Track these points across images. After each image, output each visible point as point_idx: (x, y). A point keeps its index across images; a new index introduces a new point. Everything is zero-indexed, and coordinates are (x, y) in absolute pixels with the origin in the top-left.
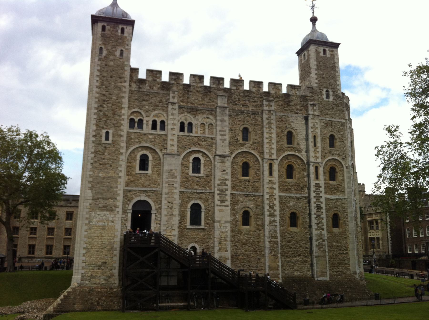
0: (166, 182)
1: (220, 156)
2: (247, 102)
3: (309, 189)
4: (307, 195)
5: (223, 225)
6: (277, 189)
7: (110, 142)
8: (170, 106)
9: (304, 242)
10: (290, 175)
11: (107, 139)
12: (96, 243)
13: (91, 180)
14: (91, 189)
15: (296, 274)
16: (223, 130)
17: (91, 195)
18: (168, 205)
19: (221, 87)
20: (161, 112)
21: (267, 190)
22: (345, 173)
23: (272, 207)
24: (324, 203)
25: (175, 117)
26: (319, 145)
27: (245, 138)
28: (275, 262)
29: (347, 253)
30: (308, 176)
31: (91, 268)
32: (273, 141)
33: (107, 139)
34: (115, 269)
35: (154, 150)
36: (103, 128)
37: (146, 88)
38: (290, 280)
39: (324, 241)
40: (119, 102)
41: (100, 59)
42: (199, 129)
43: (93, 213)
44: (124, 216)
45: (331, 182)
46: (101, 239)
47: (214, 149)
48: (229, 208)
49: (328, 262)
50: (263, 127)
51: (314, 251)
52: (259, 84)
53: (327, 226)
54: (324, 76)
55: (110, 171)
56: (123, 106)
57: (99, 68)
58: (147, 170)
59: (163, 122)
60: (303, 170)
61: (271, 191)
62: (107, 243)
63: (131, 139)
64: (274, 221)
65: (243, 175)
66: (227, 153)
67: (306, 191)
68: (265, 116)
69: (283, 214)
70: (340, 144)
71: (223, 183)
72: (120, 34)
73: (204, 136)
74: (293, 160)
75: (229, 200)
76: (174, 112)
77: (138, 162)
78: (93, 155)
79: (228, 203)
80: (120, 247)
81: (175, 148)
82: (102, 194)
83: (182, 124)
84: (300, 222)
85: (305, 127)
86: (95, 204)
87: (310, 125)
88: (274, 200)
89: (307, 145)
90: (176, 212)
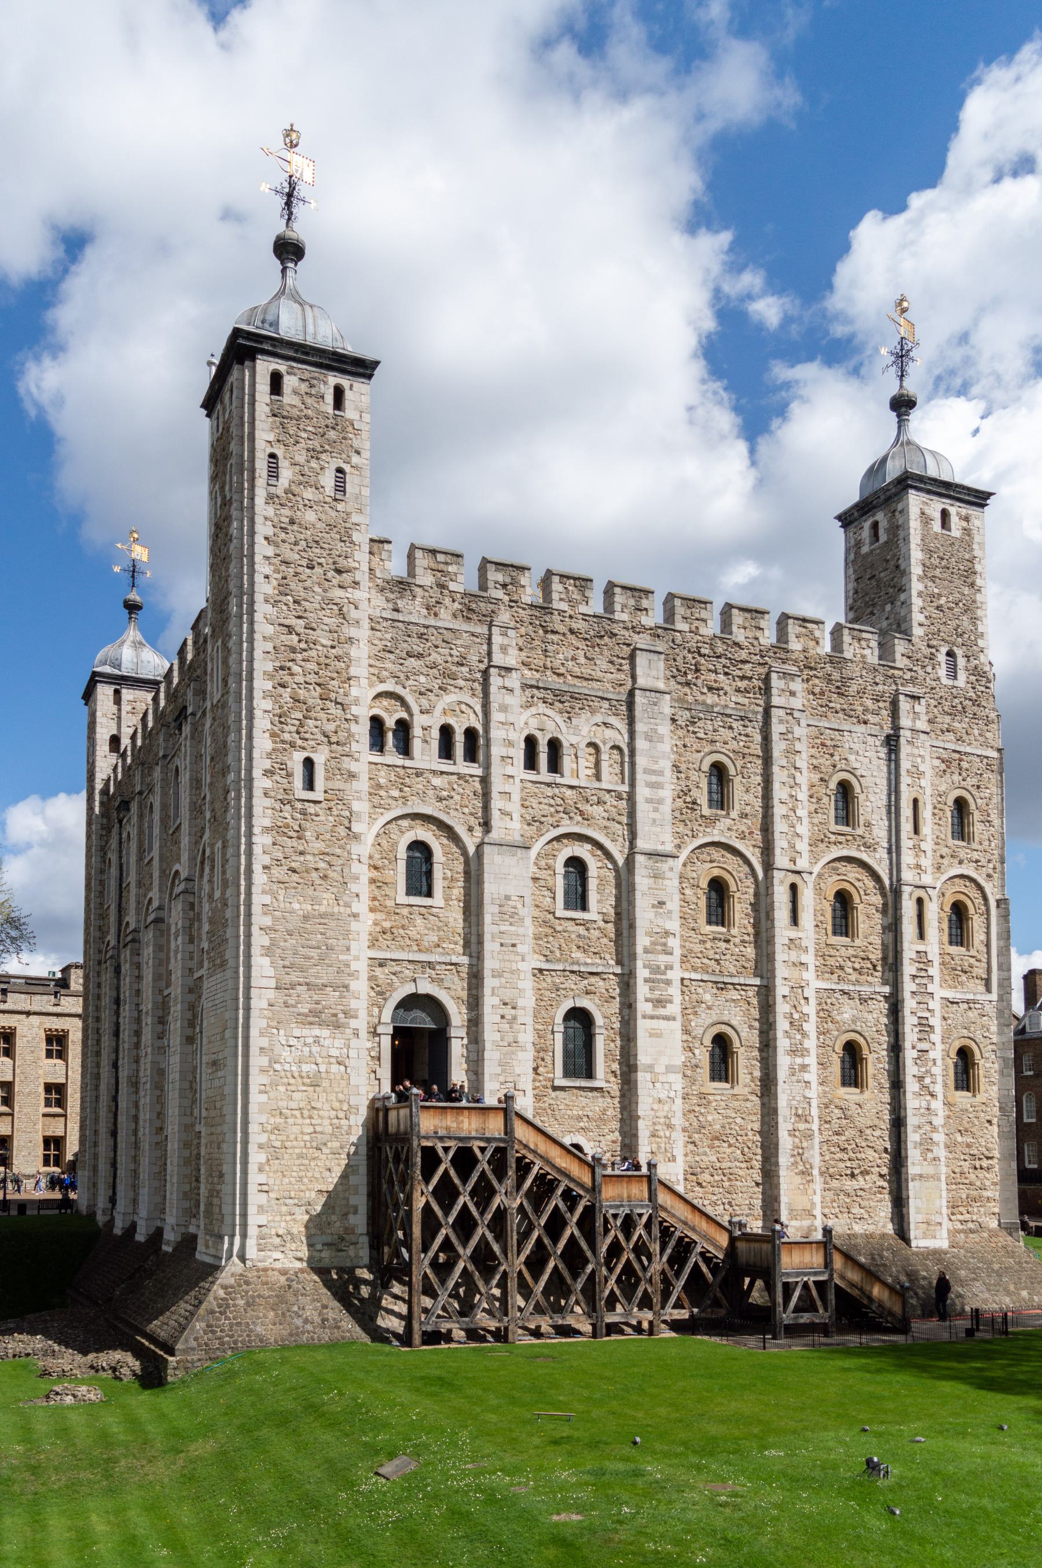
1: (650, 855)
6: (812, 968)
12: (296, 1129)
13: (270, 924)
14: (268, 952)
15: (858, 1228)
16: (655, 767)
17: (271, 972)
18: (501, 1012)
20: (466, 698)
23: (796, 1025)
24: (938, 1014)
26: (926, 829)
31: (284, 1209)
32: (799, 813)
34: (356, 1212)
39: (935, 1129)
43: (282, 1032)
45: (955, 950)
46: (311, 1117)
48: (677, 1025)
51: (910, 1160)
53: (945, 1085)
55: (325, 895)
58: (429, 894)
63: (380, 786)
64: (804, 1068)
66: (669, 848)
68: (777, 728)
73: (597, 785)
74: (853, 873)
75: (677, 999)
77: (402, 866)
79: (674, 1009)
80: (368, 1143)
83: (531, 742)
86: (286, 1005)
88: (802, 1002)
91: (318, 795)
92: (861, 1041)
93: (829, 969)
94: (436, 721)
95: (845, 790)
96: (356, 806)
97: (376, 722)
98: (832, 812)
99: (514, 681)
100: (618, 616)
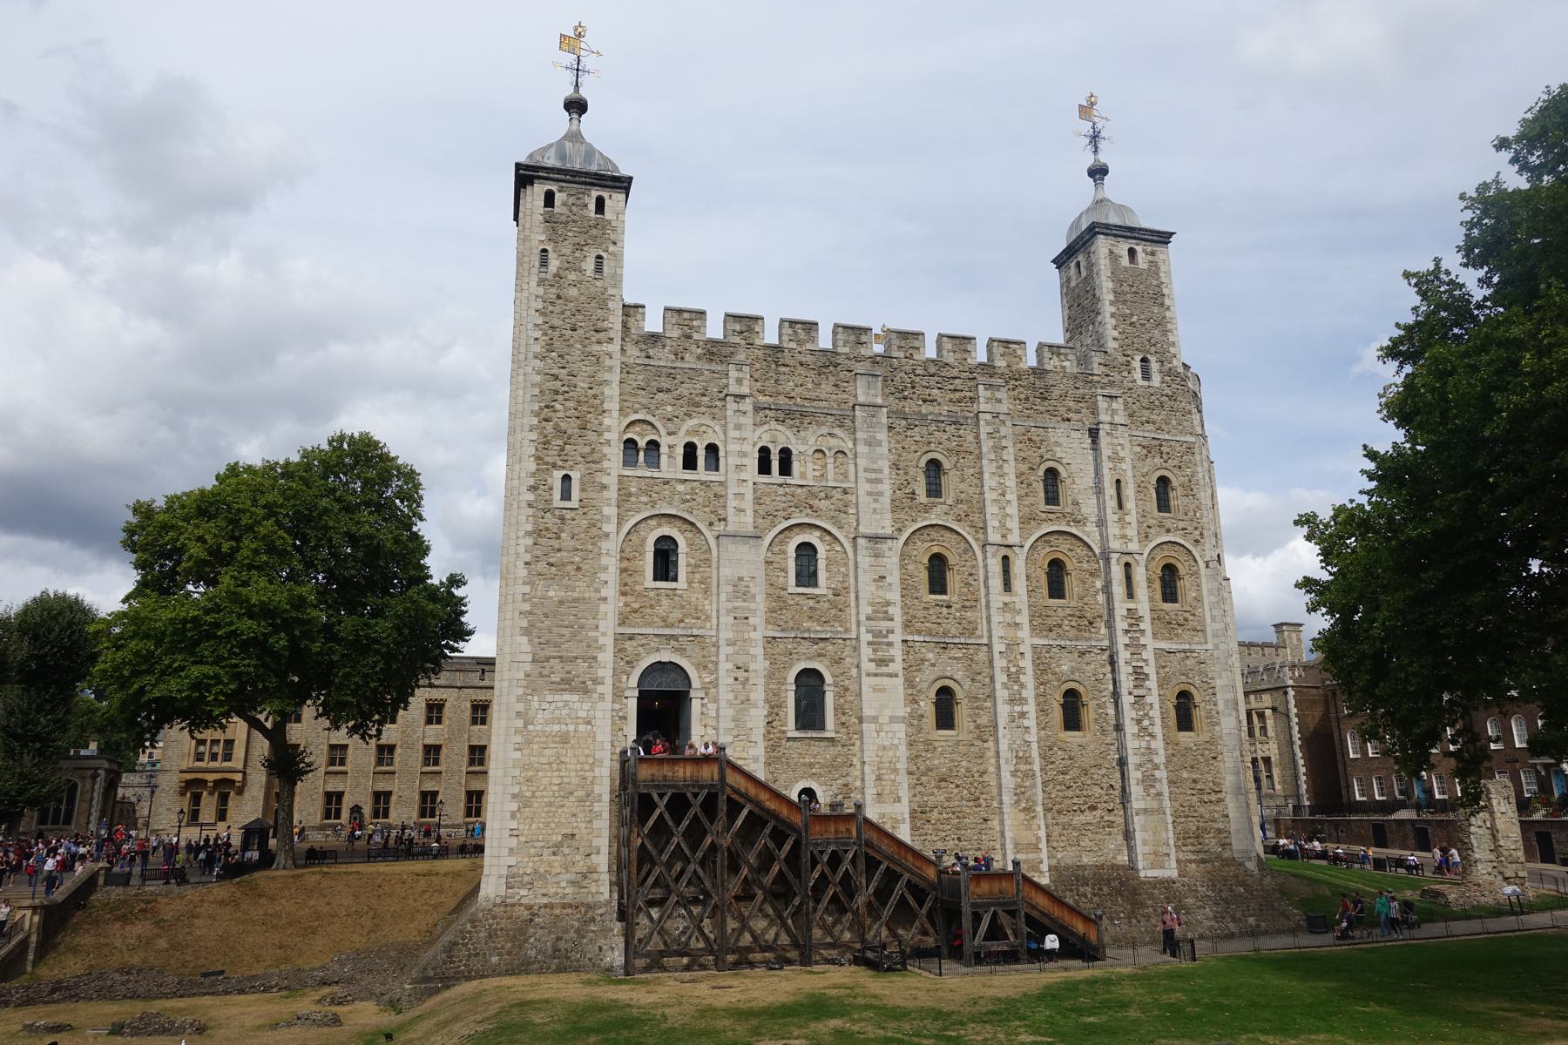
0: (728, 611)
2: (936, 391)
3: (1110, 625)
4: (1106, 643)
5: (886, 728)
6: (1026, 626)
7: (574, 503)
8: (731, 405)
9: (1104, 771)
10: (1057, 590)
11: (566, 496)
14: (526, 632)
15: (1086, 860)
17: (528, 648)
19: (863, 351)
21: (998, 632)
22: (1203, 579)
23: (1014, 677)
24: (1152, 662)
25: (745, 435)
26: (1130, 505)
27: (934, 491)
28: (1029, 827)
29: (1220, 801)
30: (1107, 589)
32: (1008, 497)
33: (566, 496)
35: (692, 524)
36: (554, 466)
37: (663, 357)
38: (1069, 876)
39: (1156, 767)
40: (595, 397)
41: (541, 282)
42: (810, 466)
44: (617, 706)
45: (1168, 606)
47: (852, 519)
48: (900, 681)
49: (1170, 826)
50: (980, 457)
52: (963, 342)
53: (1165, 726)
54: (1134, 319)
56: (606, 406)
57: (540, 305)
58: (675, 579)
59: (712, 449)
60: (1091, 574)
61: (1011, 632)
62: (575, 781)
63: (630, 495)
64: (1023, 715)
65: (932, 591)
66: (889, 531)
67: (1103, 630)
68: (984, 429)
69: (1044, 695)
70: (1186, 500)
71: (881, 611)
72: (593, 214)
74: (1064, 545)
75: (899, 659)
76: (742, 420)
78: (530, 541)
79: (897, 667)
81: (747, 521)
82: (557, 645)
83: (764, 453)
84: (1089, 715)
85: (1091, 458)
87: (1106, 452)
89: (1101, 507)
90: (758, 695)
91: (574, 503)
92: (1081, 689)
93: (1043, 625)
94: (680, 442)
95: (1052, 474)
96: (607, 511)
97: (630, 444)
98: (1042, 495)
99: (747, 405)
100: (840, 350)
